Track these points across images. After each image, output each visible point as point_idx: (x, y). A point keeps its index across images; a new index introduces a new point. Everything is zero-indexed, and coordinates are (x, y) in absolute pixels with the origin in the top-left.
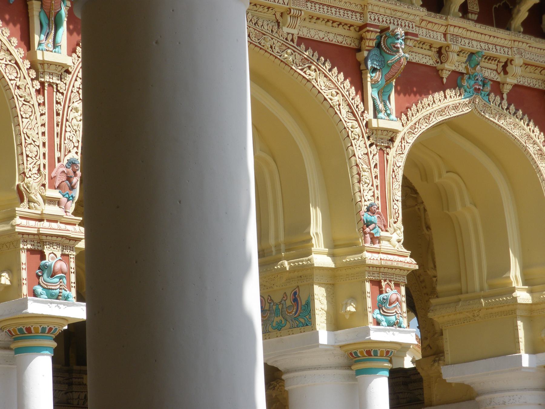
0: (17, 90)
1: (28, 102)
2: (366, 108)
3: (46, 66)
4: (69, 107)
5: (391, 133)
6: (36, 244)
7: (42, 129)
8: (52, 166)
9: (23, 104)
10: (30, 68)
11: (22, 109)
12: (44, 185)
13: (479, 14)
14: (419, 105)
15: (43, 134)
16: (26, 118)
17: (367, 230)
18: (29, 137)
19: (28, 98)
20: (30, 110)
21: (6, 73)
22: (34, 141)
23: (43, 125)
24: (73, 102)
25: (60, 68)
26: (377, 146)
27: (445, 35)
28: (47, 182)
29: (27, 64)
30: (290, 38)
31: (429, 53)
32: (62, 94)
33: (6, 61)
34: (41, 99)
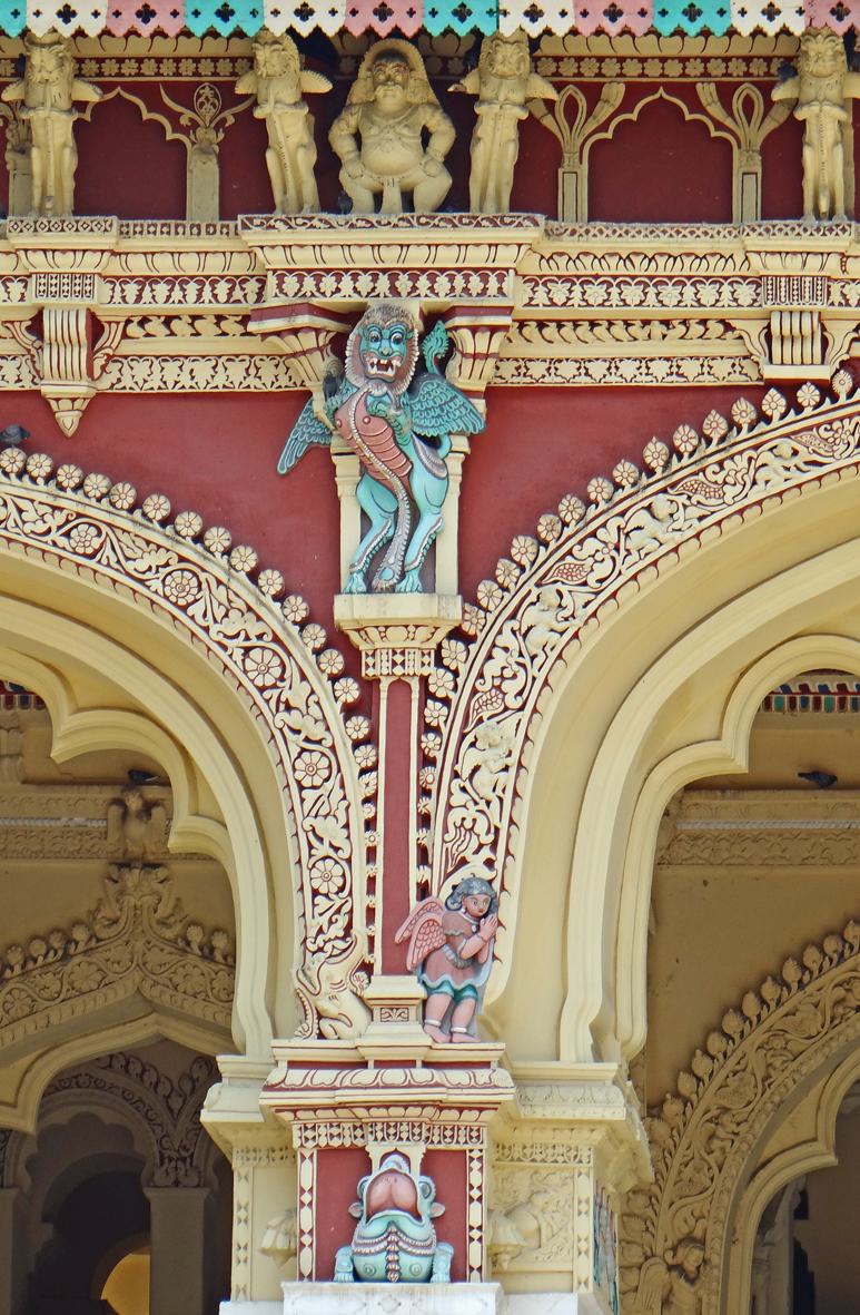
0: (283, 715)
1: (319, 742)
3: (373, 633)
4: (463, 736)
6: (347, 1133)
7: (368, 811)
8: (396, 910)
9: (303, 750)
10: (327, 646)
11: (299, 764)
12: (367, 968)
16: (313, 787)
18: (321, 840)
19: (317, 732)
20: (325, 762)
21: (245, 672)
22: (337, 849)
23: (370, 800)
24: (480, 721)
25: (422, 633)
28: (377, 959)
29: (317, 635)
32: (446, 701)
33: (247, 638)
34: (360, 726)
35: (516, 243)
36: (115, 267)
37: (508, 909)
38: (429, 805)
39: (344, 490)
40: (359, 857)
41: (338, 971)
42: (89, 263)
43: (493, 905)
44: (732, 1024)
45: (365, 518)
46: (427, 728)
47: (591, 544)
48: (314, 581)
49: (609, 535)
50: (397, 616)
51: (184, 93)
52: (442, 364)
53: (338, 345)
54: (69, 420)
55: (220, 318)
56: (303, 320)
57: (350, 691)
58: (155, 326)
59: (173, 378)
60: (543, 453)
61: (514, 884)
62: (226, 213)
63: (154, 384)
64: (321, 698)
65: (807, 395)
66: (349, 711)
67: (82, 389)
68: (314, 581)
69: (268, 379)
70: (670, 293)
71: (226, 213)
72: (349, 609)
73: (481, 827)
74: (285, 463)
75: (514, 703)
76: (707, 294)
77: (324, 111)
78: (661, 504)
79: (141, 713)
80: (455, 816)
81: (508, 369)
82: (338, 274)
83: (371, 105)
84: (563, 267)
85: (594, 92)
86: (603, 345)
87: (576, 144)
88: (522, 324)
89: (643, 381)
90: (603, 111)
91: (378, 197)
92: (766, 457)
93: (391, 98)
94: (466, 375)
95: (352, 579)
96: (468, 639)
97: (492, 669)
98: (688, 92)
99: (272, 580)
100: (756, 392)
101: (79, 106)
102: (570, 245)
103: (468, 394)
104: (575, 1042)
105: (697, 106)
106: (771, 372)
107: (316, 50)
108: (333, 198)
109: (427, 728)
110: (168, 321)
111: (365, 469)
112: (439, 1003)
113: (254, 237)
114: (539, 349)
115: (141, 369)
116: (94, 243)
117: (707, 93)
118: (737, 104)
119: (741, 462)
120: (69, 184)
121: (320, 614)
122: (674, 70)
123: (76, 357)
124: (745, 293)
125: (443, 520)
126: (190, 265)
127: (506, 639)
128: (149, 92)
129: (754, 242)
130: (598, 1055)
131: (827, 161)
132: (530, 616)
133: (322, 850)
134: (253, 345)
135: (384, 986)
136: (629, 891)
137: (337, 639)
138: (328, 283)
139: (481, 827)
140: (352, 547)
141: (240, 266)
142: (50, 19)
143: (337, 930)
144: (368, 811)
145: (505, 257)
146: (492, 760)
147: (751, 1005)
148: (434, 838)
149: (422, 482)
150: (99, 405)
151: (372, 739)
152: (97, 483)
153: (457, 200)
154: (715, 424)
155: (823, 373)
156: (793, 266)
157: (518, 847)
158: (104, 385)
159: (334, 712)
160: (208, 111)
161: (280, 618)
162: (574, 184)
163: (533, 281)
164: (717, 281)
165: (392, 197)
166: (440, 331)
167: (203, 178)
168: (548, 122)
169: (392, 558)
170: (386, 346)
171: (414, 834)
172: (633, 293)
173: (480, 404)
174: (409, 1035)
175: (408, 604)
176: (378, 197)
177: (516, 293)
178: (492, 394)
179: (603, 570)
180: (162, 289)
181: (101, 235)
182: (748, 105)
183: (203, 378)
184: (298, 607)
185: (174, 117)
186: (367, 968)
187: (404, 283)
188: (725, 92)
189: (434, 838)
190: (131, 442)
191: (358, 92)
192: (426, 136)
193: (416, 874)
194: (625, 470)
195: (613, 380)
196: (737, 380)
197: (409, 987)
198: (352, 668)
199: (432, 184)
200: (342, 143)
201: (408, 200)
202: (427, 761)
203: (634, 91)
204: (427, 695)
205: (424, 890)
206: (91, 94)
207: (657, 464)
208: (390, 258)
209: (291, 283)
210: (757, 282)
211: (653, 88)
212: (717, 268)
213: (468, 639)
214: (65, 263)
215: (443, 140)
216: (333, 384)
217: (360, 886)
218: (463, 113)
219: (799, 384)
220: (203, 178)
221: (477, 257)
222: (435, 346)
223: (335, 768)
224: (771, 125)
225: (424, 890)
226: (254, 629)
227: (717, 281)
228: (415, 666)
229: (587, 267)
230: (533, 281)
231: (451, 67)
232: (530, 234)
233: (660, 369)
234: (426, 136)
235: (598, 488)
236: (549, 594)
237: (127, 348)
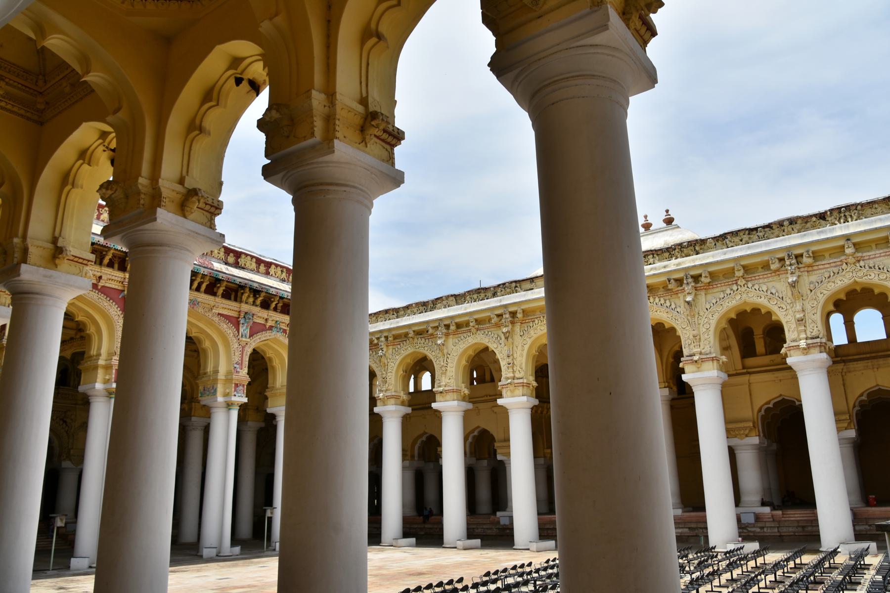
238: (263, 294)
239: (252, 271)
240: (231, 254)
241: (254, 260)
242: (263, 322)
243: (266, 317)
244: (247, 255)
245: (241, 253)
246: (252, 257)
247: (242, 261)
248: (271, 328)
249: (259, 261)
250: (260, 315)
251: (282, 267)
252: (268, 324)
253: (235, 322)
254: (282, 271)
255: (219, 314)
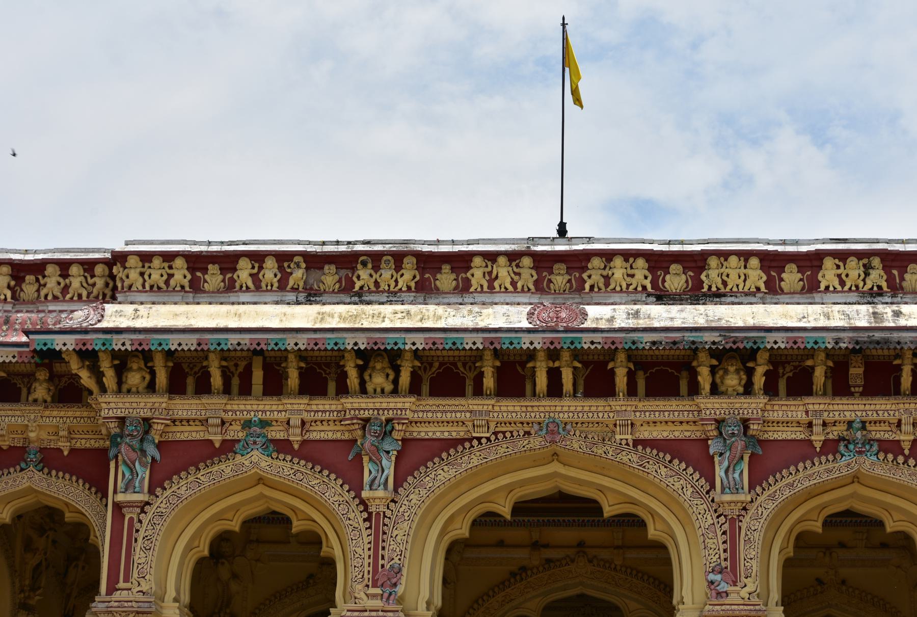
2: (713, 486)
5: (739, 504)
7: (369, 546)
12: (368, 586)
13: (864, 386)
14: (778, 476)
15: (383, 548)
17: (712, 587)
19: (357, 525)
23: (370, 543)
26: (725, 516)
27: (807, 412)
29: (357, 501)
30: (624, 442)
31: (801, 429)
34: (367, 524)
35: (407, 402)
36: (308, 408)
37: (405, 571)
38: (384, 544)
39: (365, 464)
40: (366, 558)
41: (360, 587)
42: (302, 407)
43: (400, 570)
44: (476, 606)
45: (370, 472)
46: (384, 525)
47: (428, 478)
48: (356, 487)
49: (432, 476)
50: (377, 496)
51: (328, 365)
52: (391, 432)
53: (364, 428)
54: (296, 446)
55: (335, 421)
56: (355, 421)
57: (365, 515)
58: (318, 423)
59: (322, 436)
60: (415, 456)
61: (406, 566)
62: (337, 395)
63: (318, 437)
64: (357, 517)
65: (484, 441)
66: (365, 520)
67: (299, 438)
68: (356, 487)
69: (347, 436)
70: (449, 415)
71: (337, 395)
72: (365, 494)
73: (398, 550)
74: (350, 458)
75: (407, 518)
76: (458, 415)
77: (361, 370)
78: (446, 468)
79: (314, 521)
80: (391, 547)
81: (407, 434)
82: (364, 410)
83: (374, 368)
84: (421, 408)
85: (431, 365)
86: (432, 428)
87: (426, 378)
88: (411, 422)
89: (442, 437)
90: (434, 369)
91: (375, 390)
92: (473, 456)
93: (379, 366)
94: (395, 435)
95: (367, 487)
96: (395, 502)
97: (401, 510)
98: (455, 364)
99: (346, 487)
100: (470, 440)
101: (301, 368)
102: (423, 403)
103: (397, 440)
104: (422, 606)
105: (457, 368)
106: (475, 435)
107: (359, 353)
108: (363, 391)
109: (384, 525)
110: (322, 422)
111: (370, 459)
112: (386, 595)
113: (343, 400)
114: (415, 429)
115: (315, 434)
116: (301, 403)
117: (460, 365)
118: (467, 368)
119: (466, 458)
120: (297, 387)
121: (358, 496)
122: (451, 359)
123: (298, 431)
124: (468, 415)
125: (390, 471)
126: (327, 407)
127: (406, 502)
128: (319, 365)
129: (470, 402)
130: (428, 609)
131: (489, 382)
132: (411, 496)
133: (357, 556)
134: (343, 428)
135: (372, 591)
136: (437, 568)
137: (363, 502)
138: (362, 412)
139: (398, 550)
140: (367, 478)
141: (340, 408)
142: (292, 345)
143: (360, 576)
144: (369, 546)
145: (407, 405)
146: (401, 533)
147: (480, 602)
148: (386, 553)
149: (384, 462)
150: (304, 443)
151: (370, 528)
152: (303, 462)
153: (395, 392)
154: (460, 448)
155: (488, 435)
156: (480, 408)
157: (407, 556)
158: (305, 438)
159: (361, 521)
160: (333, 369)
161: (348, 496)
162: (425, 388)
163: (414, 412)
164: (461, 412)
165: (379, 390)
166: (390, 425)
167: (332, 387)
168: (419, 372)
169: (377, 482)
170: (376, 428)
171: (380, 552)
172: (439, 415)
173: (400, 443)
174: (377, 603)
175: (380, 493)
176: (375, 390)
177: (409, 415)
178: (403, 440)
179: (431, 485)
180: (320, 414)
181: (305, 400)
182: (470, 368)
183: (330, 436)
184: (353, 494)
185: (325, 371)
186: (368, 586)
187: (381, 412)
188: (464, 365)
189: (386, 553)
190: (311, 453)
191: (371, 364)
192: (388, 375)
193: (381, 562)
194: (436, 460)
195: (434, 437)
196: (466, 437)
197: (378, 591)
198: (366, 510)
199: (389, 387)
200: (367, 378)
201: (383, 391)
202: (384, 533)
203: (441, 364)
204: (385, 516)
205: (383, 566)
206: (303, 365)
207: (445, 458)
208: (378, 406)
209: (352, 412)
210: (471, 412)
211: (446, 363)
212: (461, 408)
213: (395, 502)
214: (296, 407)
215: (391, 377)
216: (364, 436)
217: (366, 565)
218: (397, 370)
219: (482, 438)
220: (332, 387)
221: (400, 406)
222: (389, 428)
223: (361, 535)
224: (476, 373)
225: (383, 566)
226: (341, 499)
227: (461, 412)
228: (382, 509)
229: (428, 408)
230: (414, 412)
231: (393, 357)
232: (413, 399)
233: (446, 434)
234: (388, 375)
235: (430, 464)
236: (417, 490)
237: (311, 428)
238: (762, 357)
239: (750, 296)
240: (675, 268)
241: (754, 262)
242: (799, 434)
243: (801, 416)
244: (724, 255)
245: (704, 256)
246: (745, 256)
247: (711, 277)
248: (831, 447)
249: (773, 262)
250: (786, 418)
251: (859, 255)
252: (818, 438)
253: (693, 455)
254: (867, 268)
255: (636, 442)
